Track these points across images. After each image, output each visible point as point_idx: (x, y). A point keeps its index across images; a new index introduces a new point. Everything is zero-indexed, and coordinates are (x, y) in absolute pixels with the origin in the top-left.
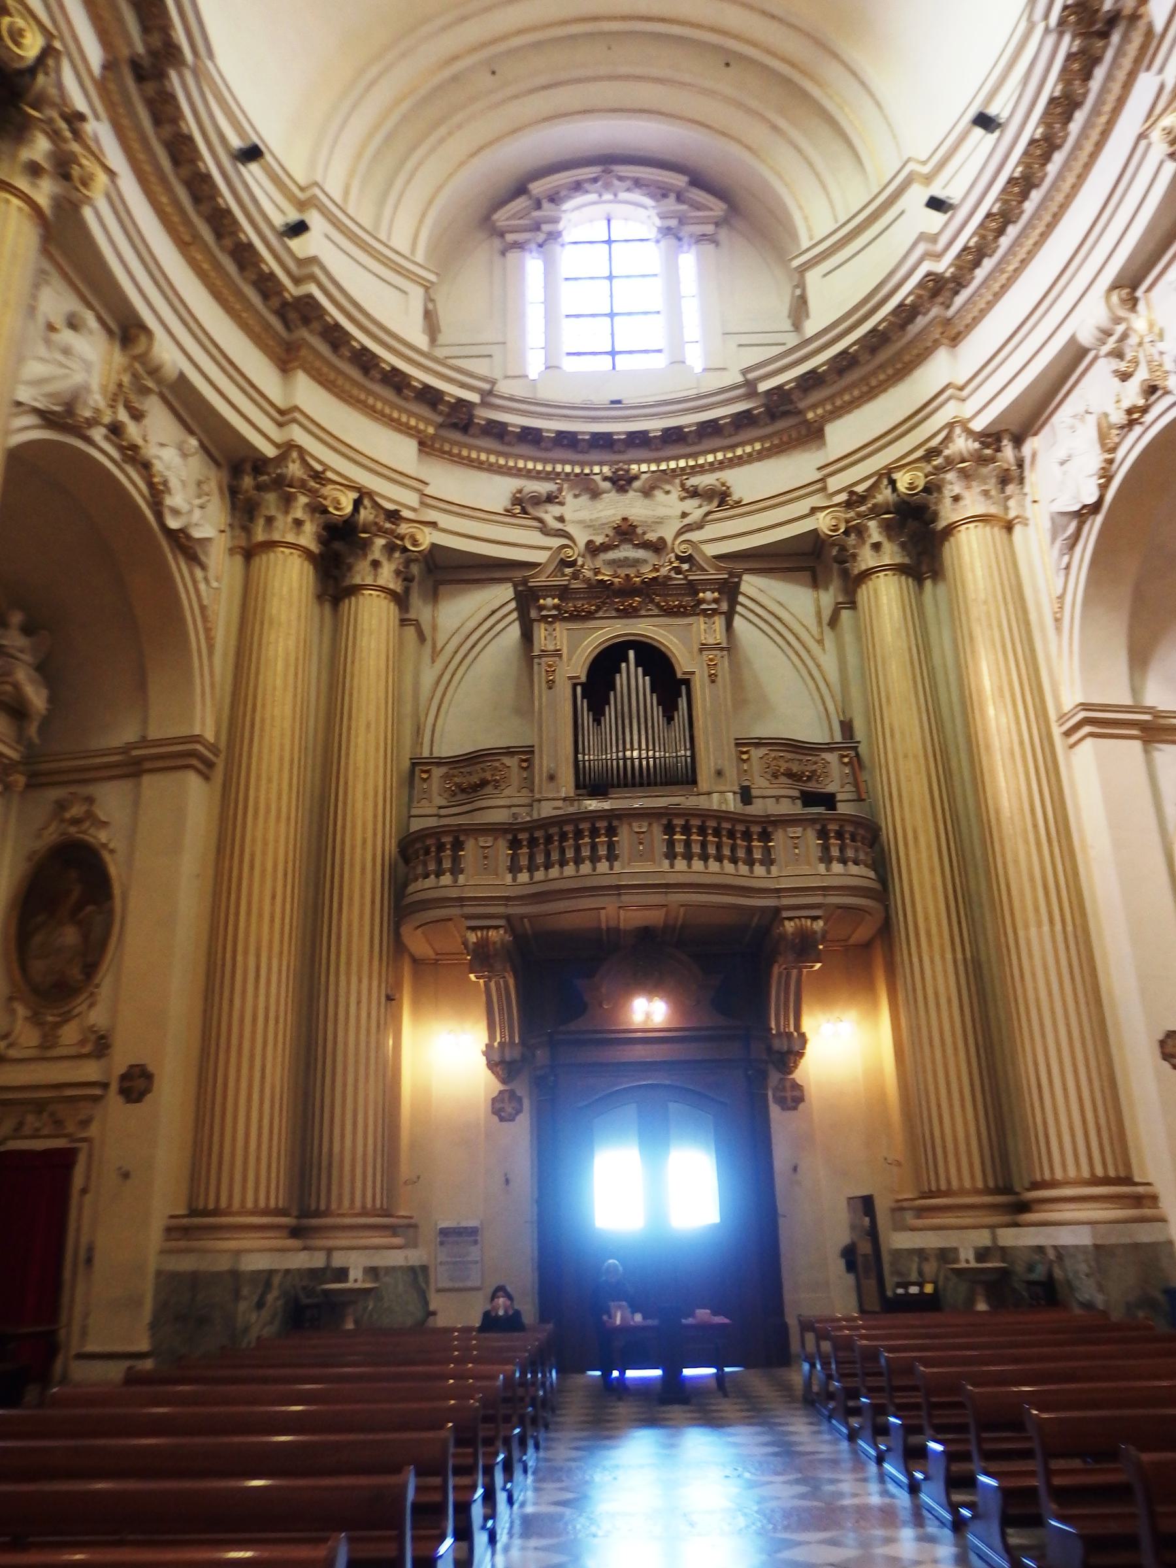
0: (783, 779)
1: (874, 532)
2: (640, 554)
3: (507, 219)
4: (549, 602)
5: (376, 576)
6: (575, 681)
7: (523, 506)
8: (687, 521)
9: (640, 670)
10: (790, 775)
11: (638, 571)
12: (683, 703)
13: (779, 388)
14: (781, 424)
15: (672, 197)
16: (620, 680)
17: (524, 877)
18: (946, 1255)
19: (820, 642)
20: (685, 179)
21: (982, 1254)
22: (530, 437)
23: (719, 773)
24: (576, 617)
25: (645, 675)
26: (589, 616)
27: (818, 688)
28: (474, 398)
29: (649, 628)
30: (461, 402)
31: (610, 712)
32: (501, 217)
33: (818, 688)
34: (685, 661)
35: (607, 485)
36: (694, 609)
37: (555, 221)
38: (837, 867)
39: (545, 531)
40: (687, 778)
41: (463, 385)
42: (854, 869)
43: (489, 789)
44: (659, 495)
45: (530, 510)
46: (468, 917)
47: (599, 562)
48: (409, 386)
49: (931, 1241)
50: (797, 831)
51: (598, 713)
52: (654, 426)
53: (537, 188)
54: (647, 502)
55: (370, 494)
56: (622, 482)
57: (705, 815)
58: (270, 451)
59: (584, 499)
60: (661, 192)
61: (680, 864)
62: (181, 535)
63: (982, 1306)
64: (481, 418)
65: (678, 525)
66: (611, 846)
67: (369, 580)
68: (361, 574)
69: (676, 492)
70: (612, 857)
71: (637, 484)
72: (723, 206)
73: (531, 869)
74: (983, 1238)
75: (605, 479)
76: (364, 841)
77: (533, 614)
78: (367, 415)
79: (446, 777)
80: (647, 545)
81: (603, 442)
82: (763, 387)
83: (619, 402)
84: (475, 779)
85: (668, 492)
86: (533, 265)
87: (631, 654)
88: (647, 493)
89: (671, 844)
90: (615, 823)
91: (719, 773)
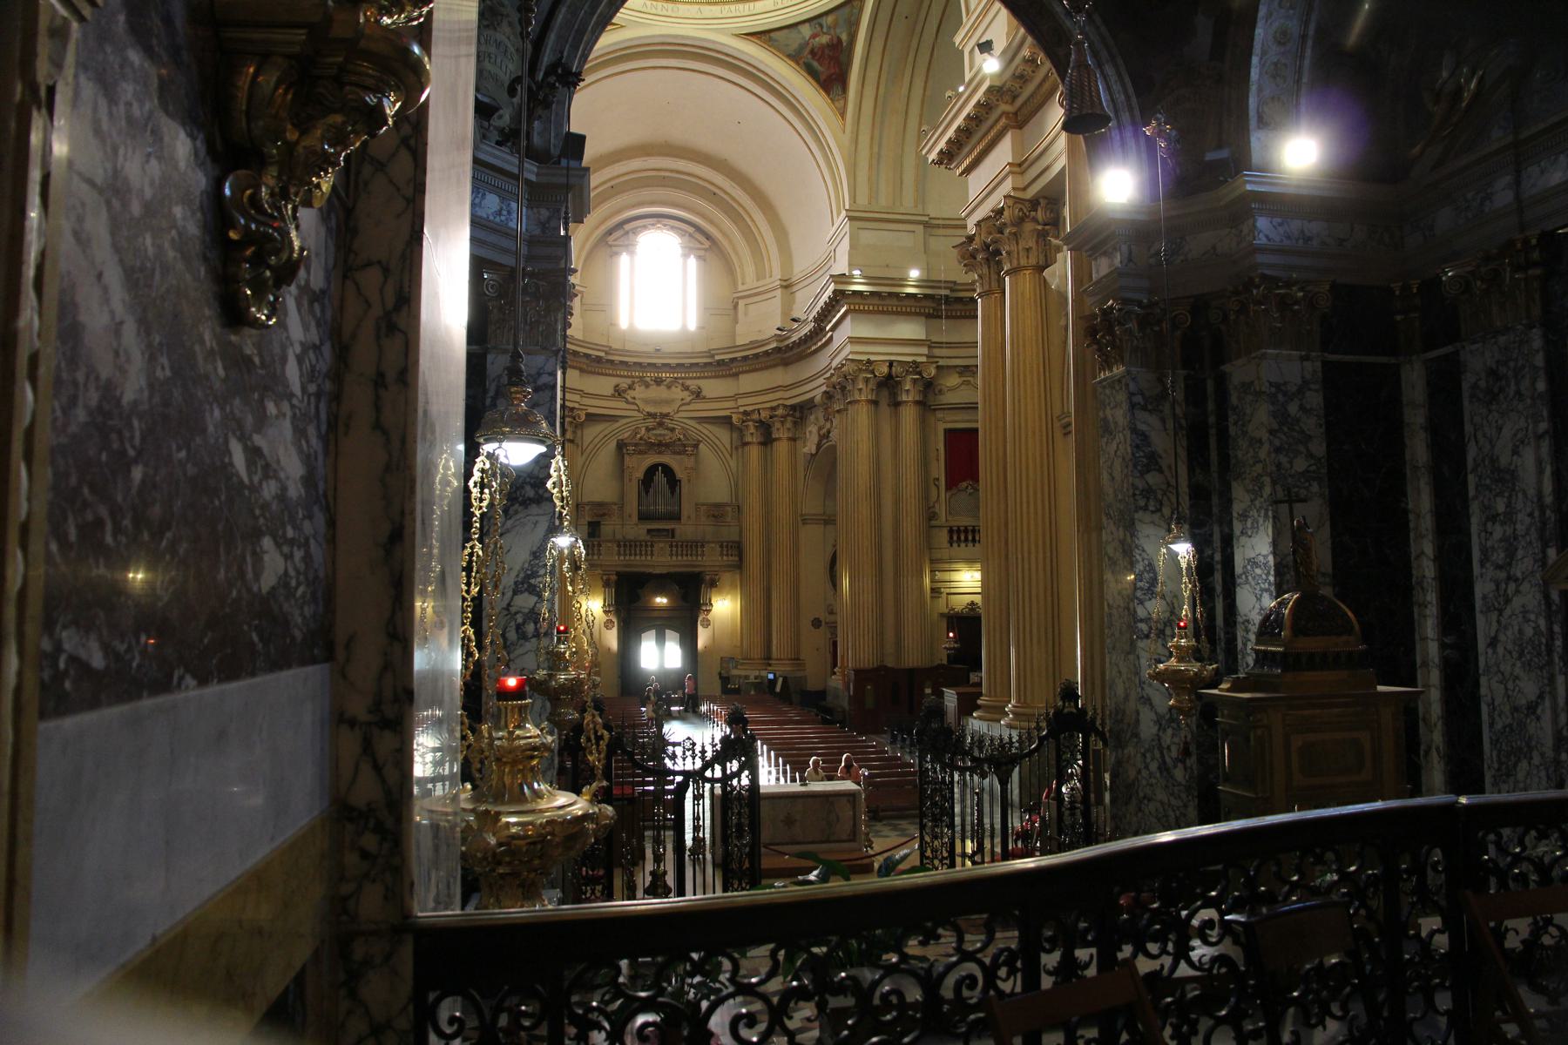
1: (752, 430)
2: (666, 432)
4: (631, 448)
7: (619, 393)
10: (714, 516)
16: (656, 478)
17: (622, 558)
18: (747, 677)
19: (731, 456)
21: (756, 678)
23: (689, 517)
24: (641, 452)
26: (646, 453)
29: (666, 459)
31: (651, 490)
32: (611, 239)
34: (679, 475)
36: (683, 452)
38: (725, 558)
39: (627, 402)
40: (676, 517)
42: (731, 558)
49: (743, 673)
52: (673, 362)
53: (627, 227)
56: (659, 382)
59: (643, 388)
60: (682, 233)
61: (674, 558)
63: (752, 693)
66: (652, 551)
69: (680, 387)
70: (652, 555)
73: (625, 555)
74: (757, 673)
77: (625, 451)
80: (667, 429)
82: (717, 358)
83: (658, 350)
84: (601, 513)
86: (624, 259)
88: (669, 387)
91: (689, 517)
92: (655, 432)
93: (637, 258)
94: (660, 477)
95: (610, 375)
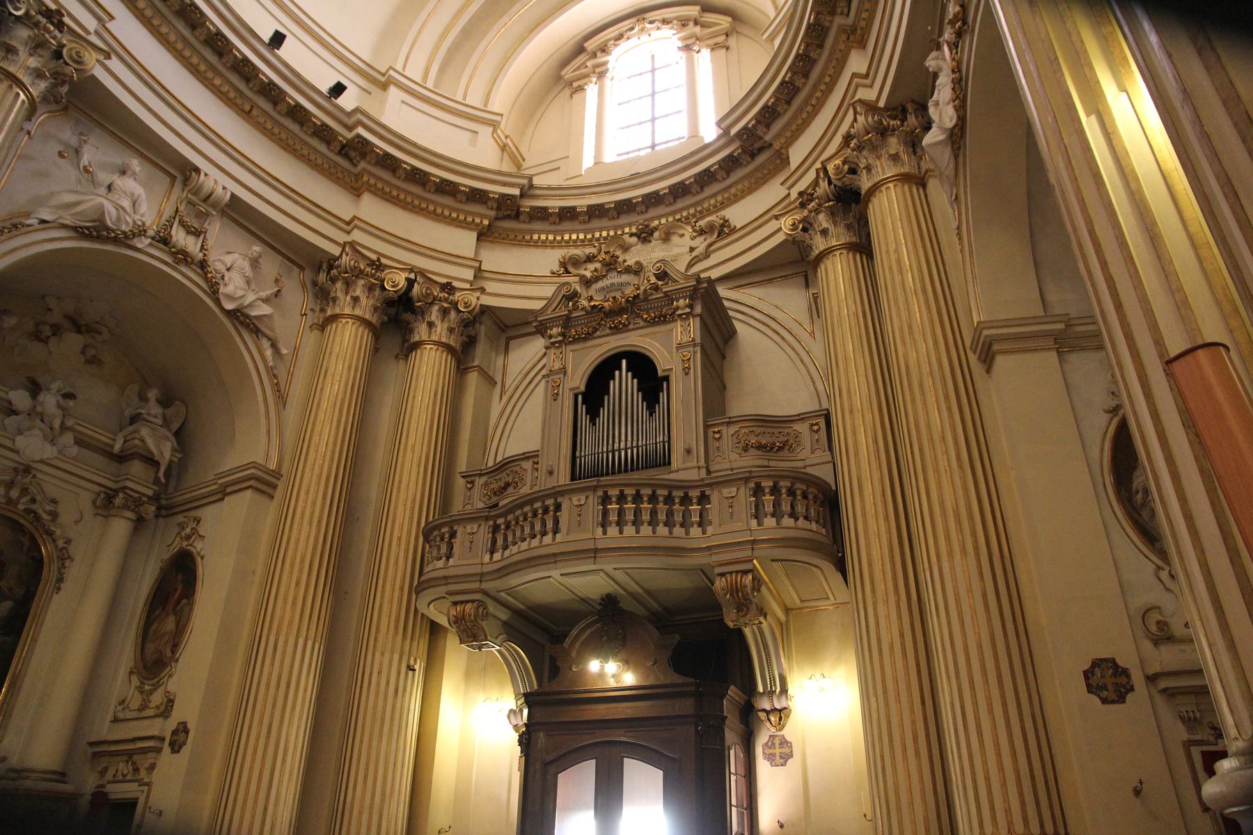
0: (752, 451)
1: (823, 220)
2: (625, 278)
3: (573, 72)
5: (430, 333)
6: (576, 391)
8: (695, 254)
9: (630, 374)
10: (760, 447)
11: (623, 292)
12: (663, 397)
13: (745, 128)
14: (761, 159)
15: (691, 24)
16: (613, 386)
19: (812, 334)
20: (698, 8)
22: (568, 214)
25: (633, 378)
27: (809, 372)
28: (516, 192)
30: (504, 197)
31: (604, 413)
32: (568, 73)
33: (809, 372)
35: (634, 239)
37: (605, 63)
41: (504, 184)
43: (510, 490)
44: (675, 239)
45: (571, 269)
46: (451, 593)
47: (592, 292)
48: (489, 198)
50: (733, 491)
51: (593, 414)
53: (591, 45)
54: (664, 246)
55: (422, 272)
57: (671, 487)
58: (336, 251)
62: (239, 314)
64: (527, 207)
65: (688, 258)
67: (425, 337)
68: (421, 332)
70: (556, 531)
71: (656, 234)
72: (729, 19)
75: (632, 235)
76: (399, 539)
78: (433, 219)
79: (486, 484)
80: (628, 270)
81: (625, 207)
85: (682, 236)
87: (624, 362)
88: (666, 238)
89: (605, 513)
90: (559, 500)
91: (688, 451)
92: (600, 284)
93: (607, 81)
94: (624, 383)
95: (544, 245)
